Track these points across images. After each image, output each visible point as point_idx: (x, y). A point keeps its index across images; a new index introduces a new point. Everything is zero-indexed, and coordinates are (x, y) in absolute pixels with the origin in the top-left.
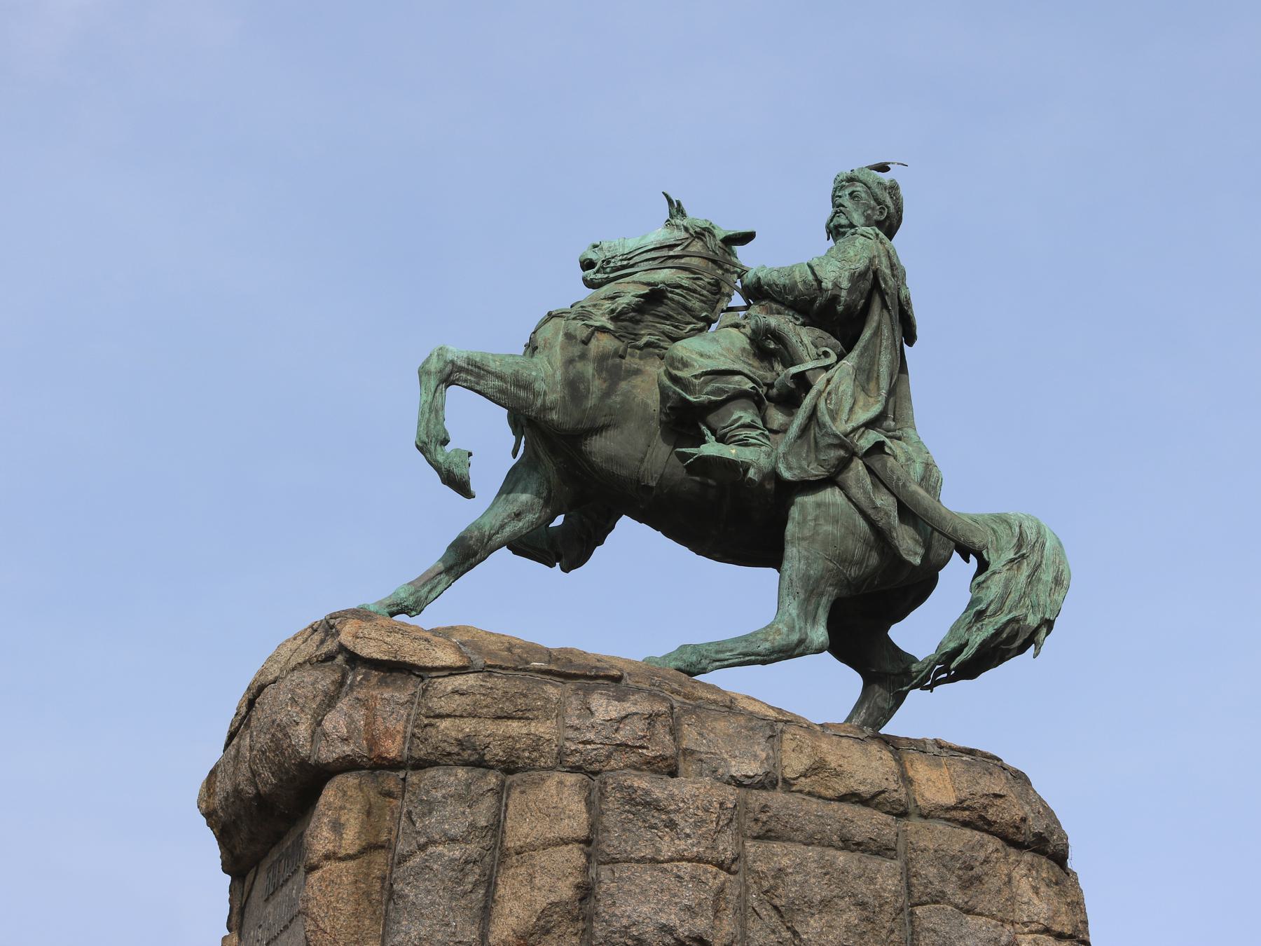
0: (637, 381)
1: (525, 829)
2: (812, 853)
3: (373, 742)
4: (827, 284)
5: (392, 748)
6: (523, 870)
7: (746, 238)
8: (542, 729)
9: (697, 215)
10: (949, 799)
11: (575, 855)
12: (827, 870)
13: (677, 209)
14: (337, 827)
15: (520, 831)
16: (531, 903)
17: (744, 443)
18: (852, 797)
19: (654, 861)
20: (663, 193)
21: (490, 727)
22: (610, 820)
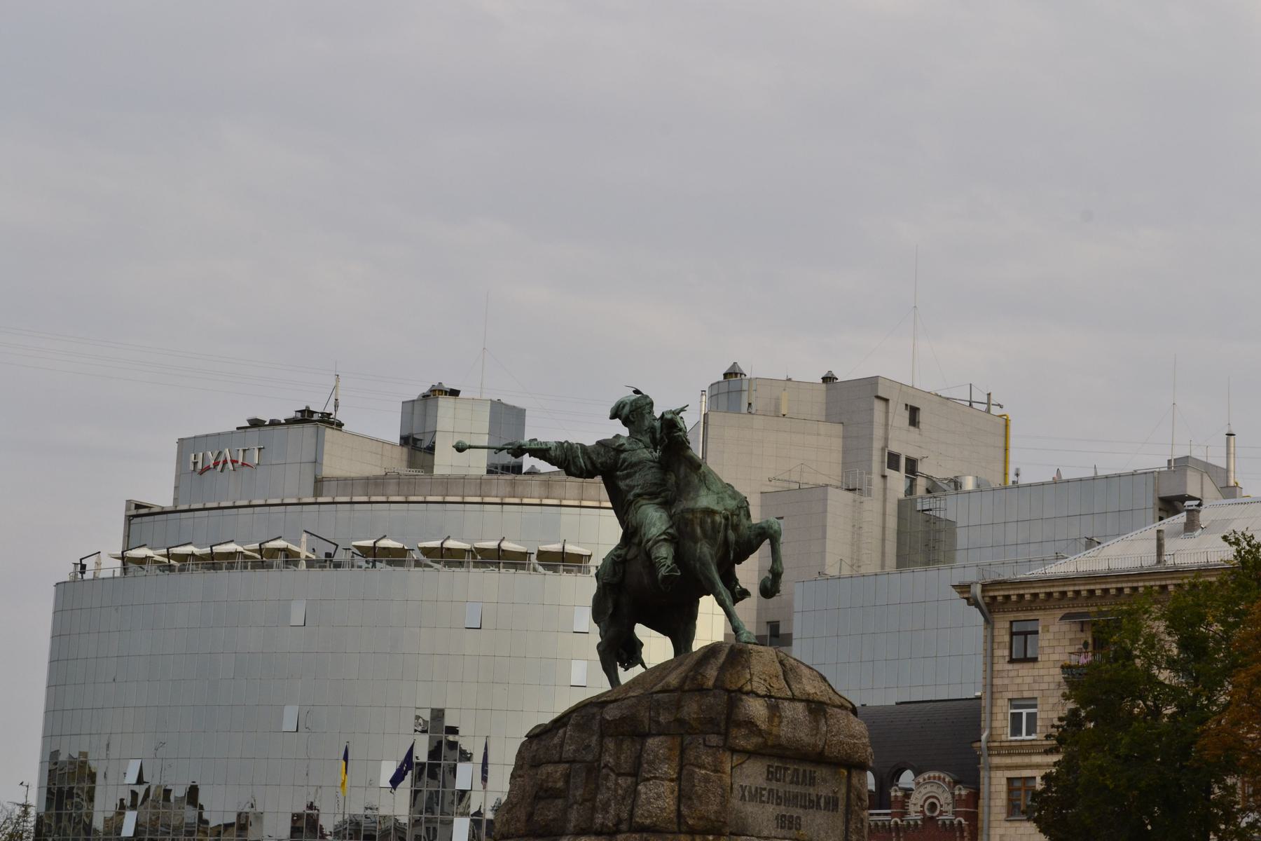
20: (688, 406)
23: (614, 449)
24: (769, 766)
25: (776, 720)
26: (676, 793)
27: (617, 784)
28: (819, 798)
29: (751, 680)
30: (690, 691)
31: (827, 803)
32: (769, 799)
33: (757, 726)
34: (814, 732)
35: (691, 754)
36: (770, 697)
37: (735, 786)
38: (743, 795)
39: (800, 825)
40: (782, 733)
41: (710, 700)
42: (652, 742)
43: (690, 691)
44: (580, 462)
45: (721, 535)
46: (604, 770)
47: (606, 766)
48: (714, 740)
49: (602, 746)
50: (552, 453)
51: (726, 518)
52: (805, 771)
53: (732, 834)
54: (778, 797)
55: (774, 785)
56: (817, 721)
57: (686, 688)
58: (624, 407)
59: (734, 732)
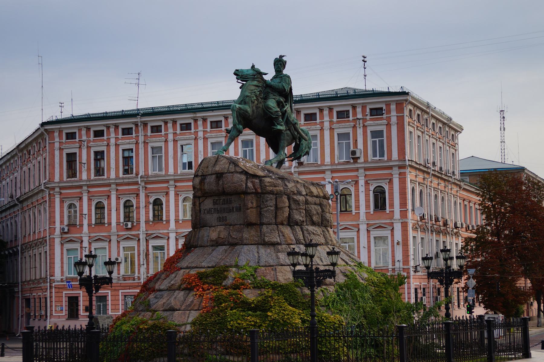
0: (260, 109)
1: (281, 205)
2: (312, 206)
3: (256, 189)
4: (287, 90)
5: (259, 191)
6: (281, 211)
7: (266, 74)
8: (282, 189)
9: (256, 67)
10: (323, 195)
11: (287, 209)
12: (315, 208)
13: (253, 67)
14: (252, 203)
15: (280, 205)
16: (283, 216)
17: (281, 125)
18: (314, 196)
19: (296, 209)
21: (274, 188)
22: (291, 203)
24: (213, 200)
25: (203, 184)
28: (233, 208)
29: (198, 171)
31: (236, 210)
32: (214, 212)
34: (217, 185)
36: (204, 175)
37: (202, 210)
38: (205, 212)
39: (226, 219)
40: (205, 188)
52: (227, 199)
54: (218, 211)
55: (216, 206)
56: (219, 180)
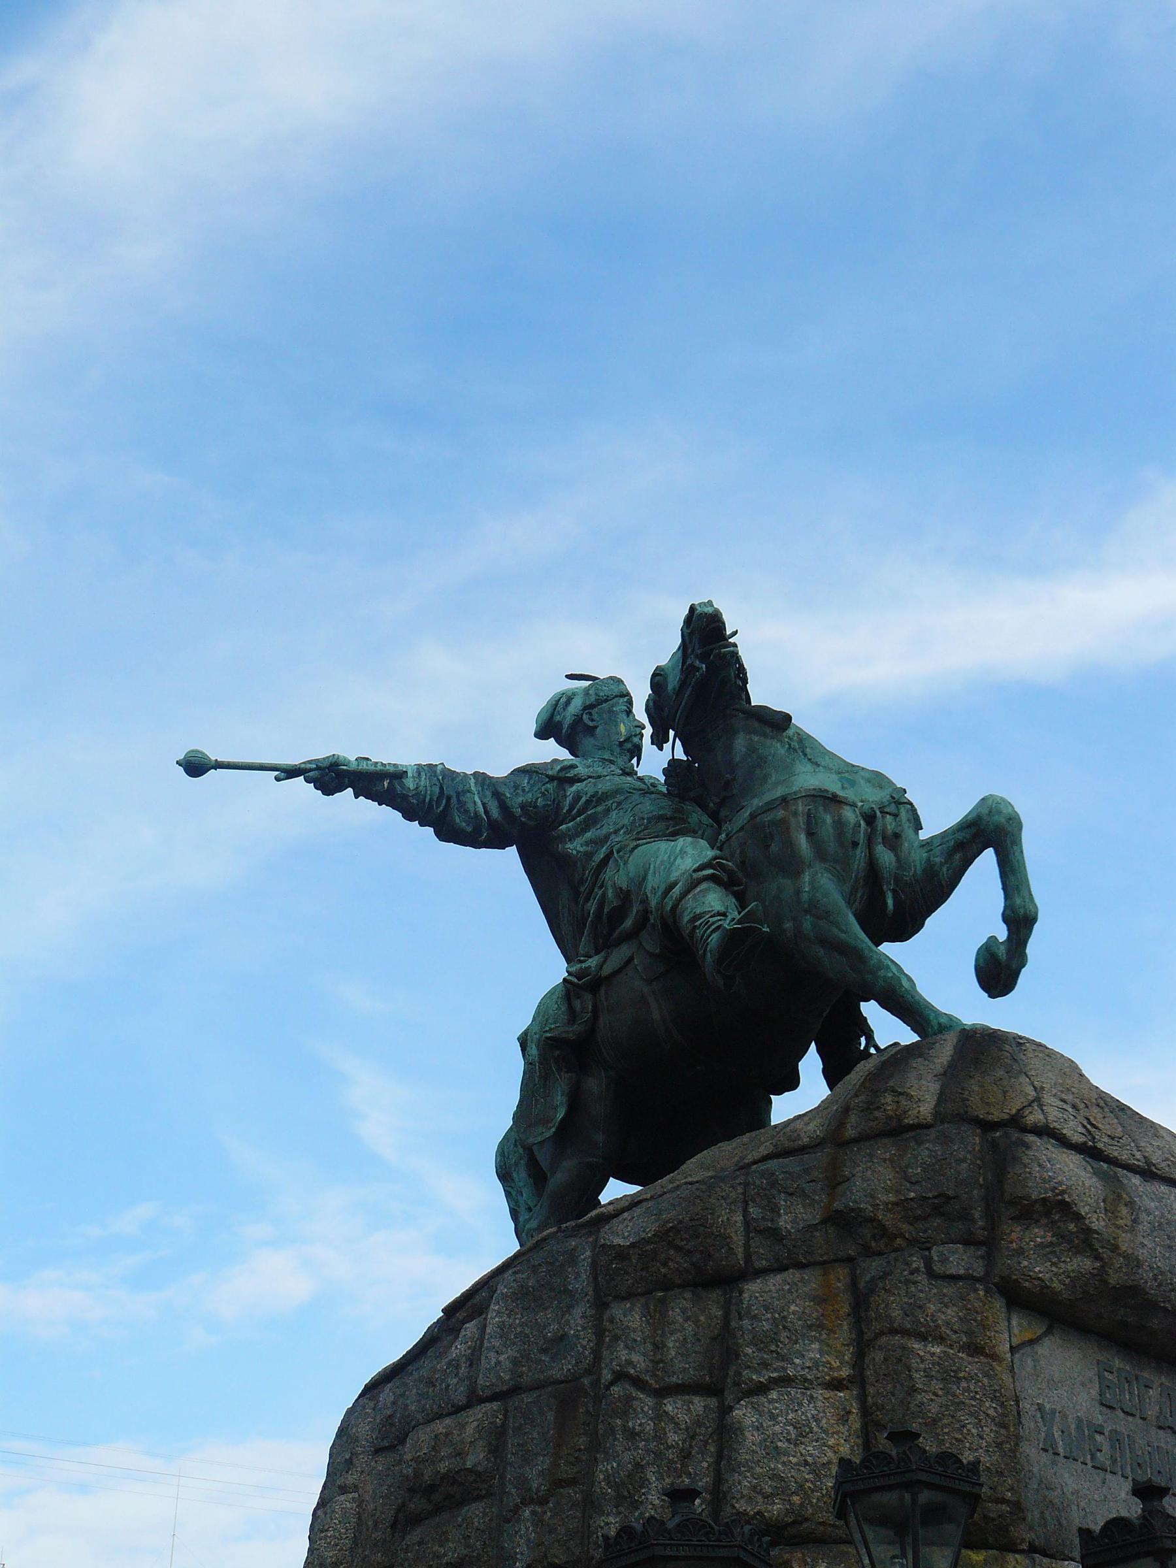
23: (552, 779)
26: (855, 1422)
27: (660, 1416)
30: (863, 1138)
33: (1078, 1217)
35: (893, 1304)
41: (927, 1150)
42: (753, 1288)
43: (863, 1138)
44: (475, 803)
45: (860, 853)
46: (615, 1389)
47: (620, 1376)
48: (958, 1260)
49: (600, 1333)
50: (410, 783)
51: (870, 818)
53: (1033, 1549)
57: (850, 1132)
58: (568, 703)
59: (1014, 1236)
